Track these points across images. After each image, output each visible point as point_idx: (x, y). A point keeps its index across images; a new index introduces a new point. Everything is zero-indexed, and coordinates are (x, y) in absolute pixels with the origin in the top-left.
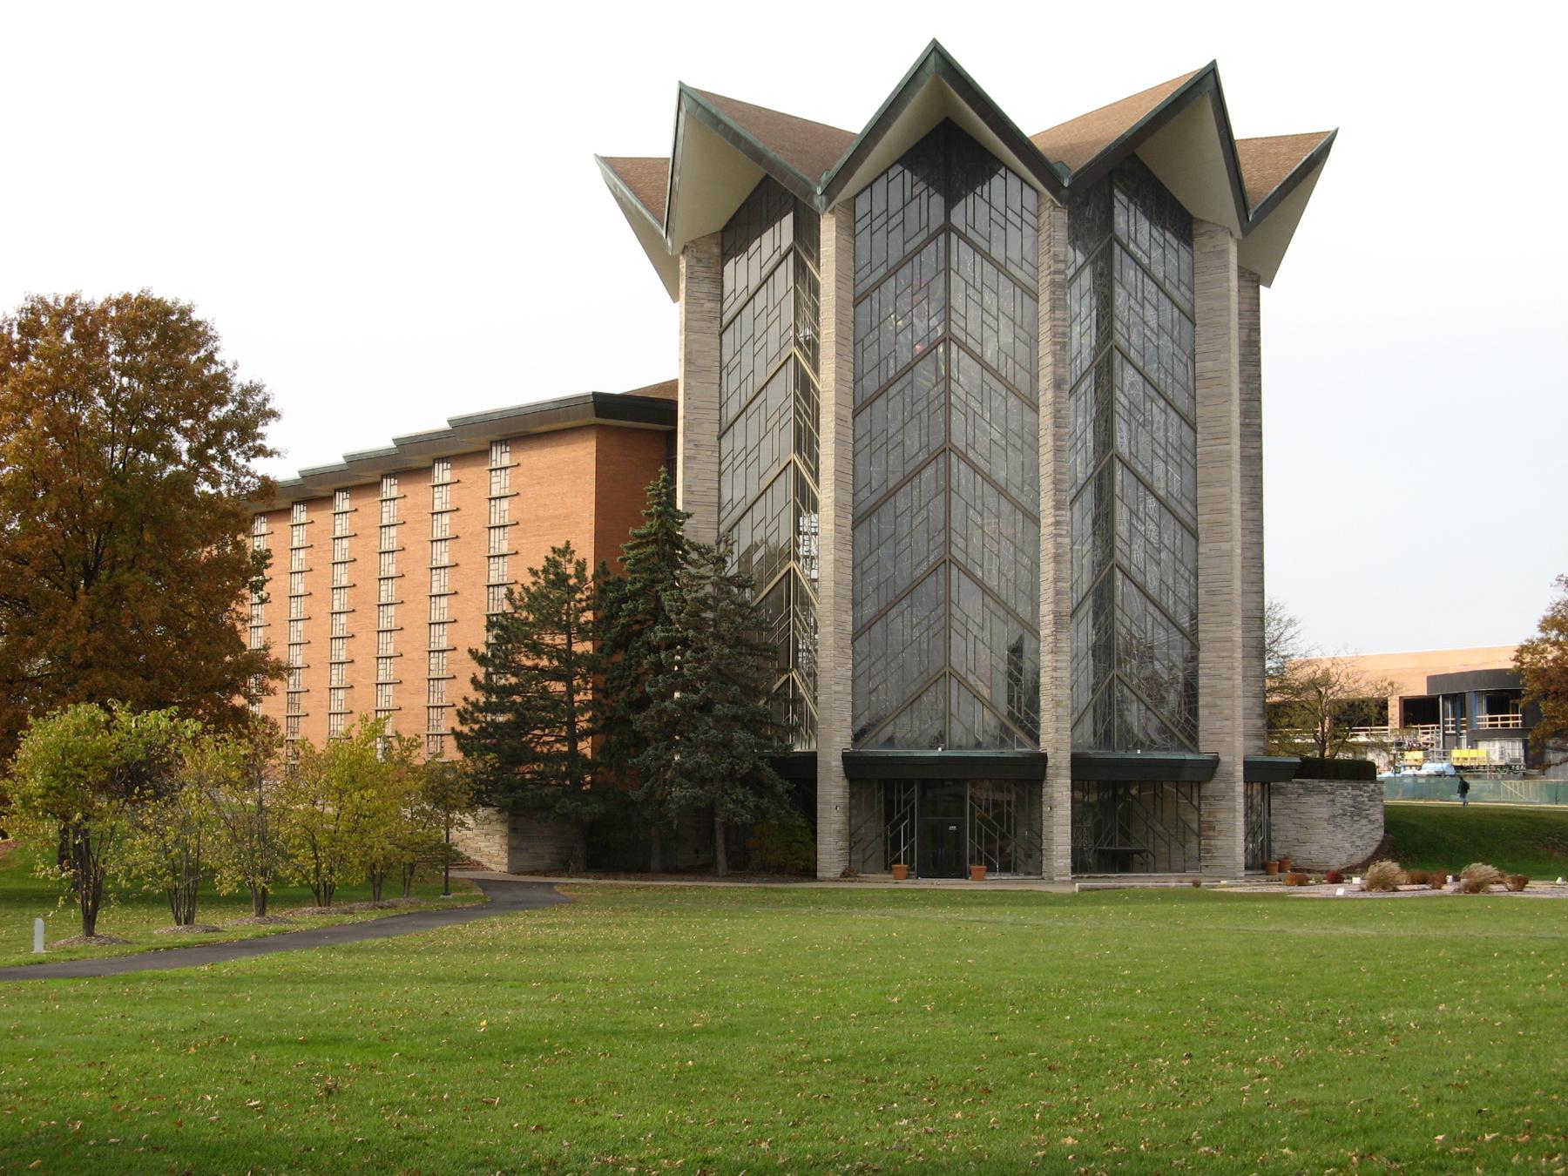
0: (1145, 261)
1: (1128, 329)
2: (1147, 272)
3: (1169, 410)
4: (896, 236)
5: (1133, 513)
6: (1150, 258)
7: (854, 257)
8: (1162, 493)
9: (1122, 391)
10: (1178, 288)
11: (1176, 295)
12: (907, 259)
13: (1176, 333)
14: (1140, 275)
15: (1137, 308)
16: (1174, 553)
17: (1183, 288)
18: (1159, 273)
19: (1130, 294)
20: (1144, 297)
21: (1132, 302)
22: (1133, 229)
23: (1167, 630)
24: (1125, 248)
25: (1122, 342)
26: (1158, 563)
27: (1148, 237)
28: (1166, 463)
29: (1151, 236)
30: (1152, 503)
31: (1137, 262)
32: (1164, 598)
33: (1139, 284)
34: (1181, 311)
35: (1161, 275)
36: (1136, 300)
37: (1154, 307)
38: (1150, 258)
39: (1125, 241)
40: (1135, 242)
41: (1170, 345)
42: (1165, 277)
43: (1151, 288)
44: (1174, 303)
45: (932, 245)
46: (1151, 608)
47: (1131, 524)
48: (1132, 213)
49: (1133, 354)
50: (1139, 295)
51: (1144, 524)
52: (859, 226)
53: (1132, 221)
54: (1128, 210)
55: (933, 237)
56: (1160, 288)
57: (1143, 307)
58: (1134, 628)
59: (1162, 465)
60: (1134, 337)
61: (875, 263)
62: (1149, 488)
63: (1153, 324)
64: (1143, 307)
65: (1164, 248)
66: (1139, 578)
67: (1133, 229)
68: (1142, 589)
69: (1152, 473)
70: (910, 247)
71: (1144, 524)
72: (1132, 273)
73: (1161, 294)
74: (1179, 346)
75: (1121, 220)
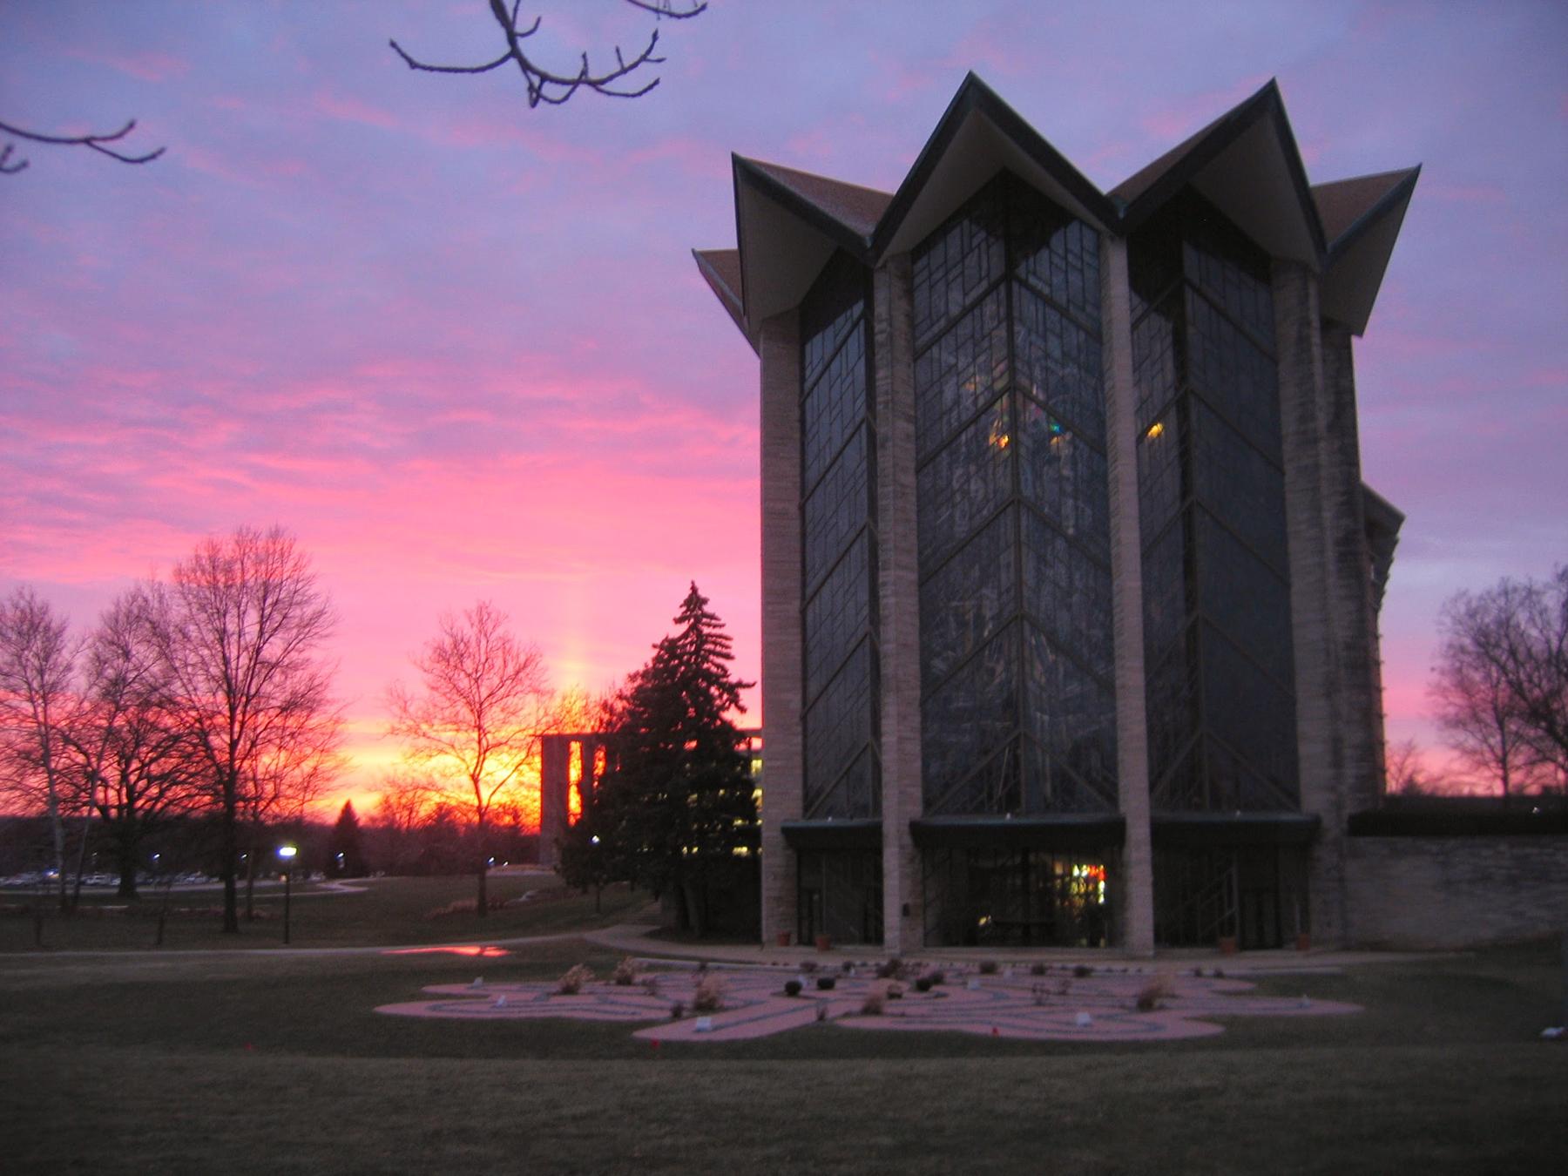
0: (1046, 291)
2: (1049, 302)
5: (1041, 559)
6: (1050, 286)
10: (1083, 309)
12: (838, 351)
14: (1040, 307)
17: (1089, 309)
18: (1061, 298)
20: (1046, 330)
21: (1033, 337)
25: (1024, 381)
26: (1069, 607)
29: (1051, 263)
31: (1036, 293)
34: (1087, 333)
35: (1064, 299)
36: (1037, 332)
38: (1050, 286)
40: (1034, 274)
41: (1075, 371)
42: (1068, 301)
43: (1054, 317)
56: (1063, 312)
57: (1045, 340)
60: (1037, 372)
63: (1057, 354)
65: (1066, 272)
72: (1032, 307)
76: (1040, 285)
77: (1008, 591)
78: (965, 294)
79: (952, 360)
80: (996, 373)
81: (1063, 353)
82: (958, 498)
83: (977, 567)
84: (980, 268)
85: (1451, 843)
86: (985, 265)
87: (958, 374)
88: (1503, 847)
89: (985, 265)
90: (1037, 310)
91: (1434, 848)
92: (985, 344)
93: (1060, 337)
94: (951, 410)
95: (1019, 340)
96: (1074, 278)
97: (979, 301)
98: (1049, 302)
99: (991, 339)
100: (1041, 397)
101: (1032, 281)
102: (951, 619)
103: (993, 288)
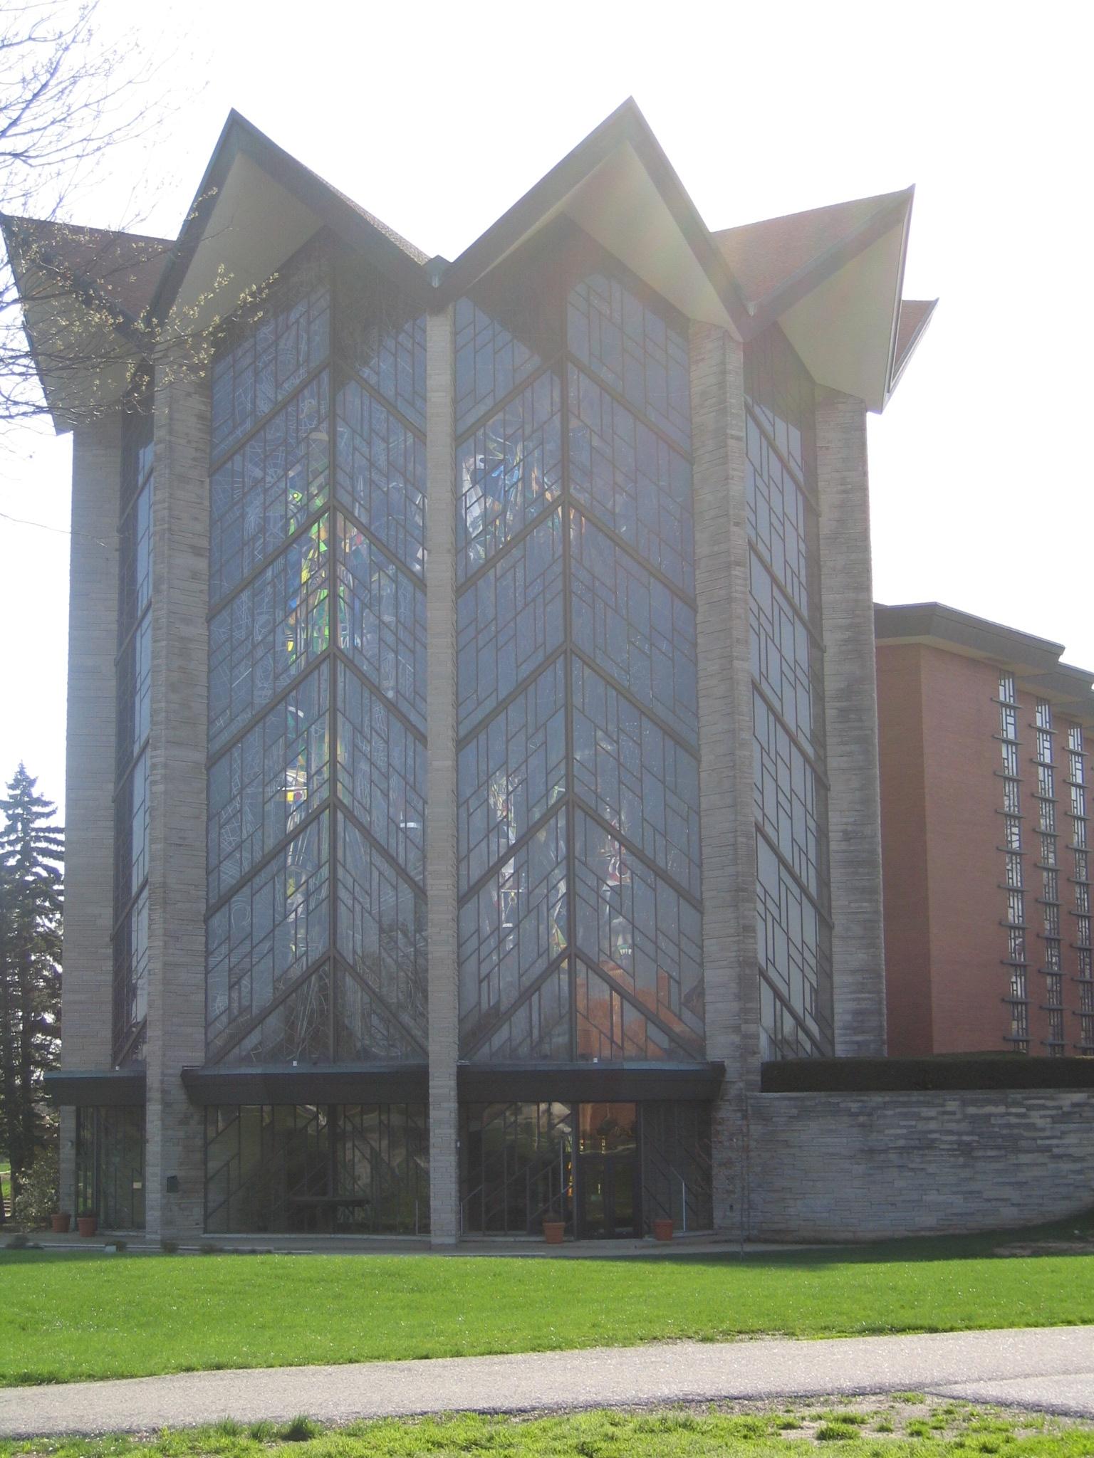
1: (352, 478)
3: (401, 578)
5: (358, 730)
8: (390, 694)
16: (404, 778)
21: (358, 440)
23: (395, 888)
25: (345, 499)
28: (396, 653)
30: (379, 710)
32: (393, 841)
36: (361, 436)
37: (383, 439)
38: (378, 374)
42: (397, 394)
46: (378, 860)
47: (355, 746)
50: (366, 427)
51: (370, 742)
57: (369, 444)
58: (357, 888)
59: (391, 656)
60: (360, 486)
62: (376, 691)
63: (382, 462)
64: (369, 444)
66: (365, 819)
68: (366, 832)
69: (378, 670)
71: (370, 742)
77: (319, 772)
78: (278, 386)
79: (258, 473)
80: (314, 490)
82: (260, 652)
83: (281, 741)
84: (298, 354)
85: (877, 1099)
86: (303, 347)
87: (265, 491)
88: (952, 1106)
89: (303, 347)
90: (362, 403)
91: (854, 1107)
92: (301, 451)
93: (386, 440)
94: (254, 538)
95: (342, 444)
97: (296, 396)
99: (308, 446)
100: (364, 520)
102: (246, 809)
103: (314, 376)
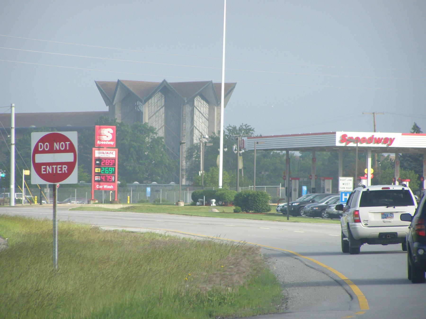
0: (200, 110)
2: (200, 112)
4: (156, 107)
6: (201, 110)
7: (149, 111)
9: (195, 134)
11: (205, 116)
12: (158, 111)
13: (205, 123)
15: (198, 119)
19: (197, 116)
20: (199, 117)
21: (197, 118)
22: (198, 104)
24: (196, 108)
27: (200, 106)
29: (201, 105)
31: (198, 110)
33: (199, 115)
34: (206, 119)
36: (198, 117)
38: (201, 110)
39: (196, 107)
40: (198, 107)
42: (203, 113)
43: (201, 115)
44: (205, 118)
45: (162, 109)
48: (198, 102)
49: (197, 127)
52: (149, 105)
53: (198, 103)
54: (197, 101)
55: (162, 107)
56: (202, 115)
57: (199, 119)
61: (152, 112)
63: (201, 122)
64: (199, 119)
67: (198, 104)
70: (158, 109)
72: (197, 113)
73: (203, 116)
74: (206, 125)
75: (196, 103)
76: (199, 109)
81: (202, 122)
96: (205, 109)
98: (200, 112)
101: (198, 108)
